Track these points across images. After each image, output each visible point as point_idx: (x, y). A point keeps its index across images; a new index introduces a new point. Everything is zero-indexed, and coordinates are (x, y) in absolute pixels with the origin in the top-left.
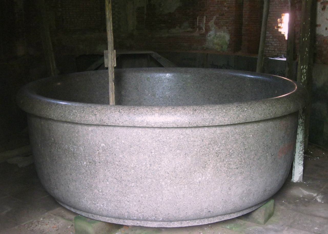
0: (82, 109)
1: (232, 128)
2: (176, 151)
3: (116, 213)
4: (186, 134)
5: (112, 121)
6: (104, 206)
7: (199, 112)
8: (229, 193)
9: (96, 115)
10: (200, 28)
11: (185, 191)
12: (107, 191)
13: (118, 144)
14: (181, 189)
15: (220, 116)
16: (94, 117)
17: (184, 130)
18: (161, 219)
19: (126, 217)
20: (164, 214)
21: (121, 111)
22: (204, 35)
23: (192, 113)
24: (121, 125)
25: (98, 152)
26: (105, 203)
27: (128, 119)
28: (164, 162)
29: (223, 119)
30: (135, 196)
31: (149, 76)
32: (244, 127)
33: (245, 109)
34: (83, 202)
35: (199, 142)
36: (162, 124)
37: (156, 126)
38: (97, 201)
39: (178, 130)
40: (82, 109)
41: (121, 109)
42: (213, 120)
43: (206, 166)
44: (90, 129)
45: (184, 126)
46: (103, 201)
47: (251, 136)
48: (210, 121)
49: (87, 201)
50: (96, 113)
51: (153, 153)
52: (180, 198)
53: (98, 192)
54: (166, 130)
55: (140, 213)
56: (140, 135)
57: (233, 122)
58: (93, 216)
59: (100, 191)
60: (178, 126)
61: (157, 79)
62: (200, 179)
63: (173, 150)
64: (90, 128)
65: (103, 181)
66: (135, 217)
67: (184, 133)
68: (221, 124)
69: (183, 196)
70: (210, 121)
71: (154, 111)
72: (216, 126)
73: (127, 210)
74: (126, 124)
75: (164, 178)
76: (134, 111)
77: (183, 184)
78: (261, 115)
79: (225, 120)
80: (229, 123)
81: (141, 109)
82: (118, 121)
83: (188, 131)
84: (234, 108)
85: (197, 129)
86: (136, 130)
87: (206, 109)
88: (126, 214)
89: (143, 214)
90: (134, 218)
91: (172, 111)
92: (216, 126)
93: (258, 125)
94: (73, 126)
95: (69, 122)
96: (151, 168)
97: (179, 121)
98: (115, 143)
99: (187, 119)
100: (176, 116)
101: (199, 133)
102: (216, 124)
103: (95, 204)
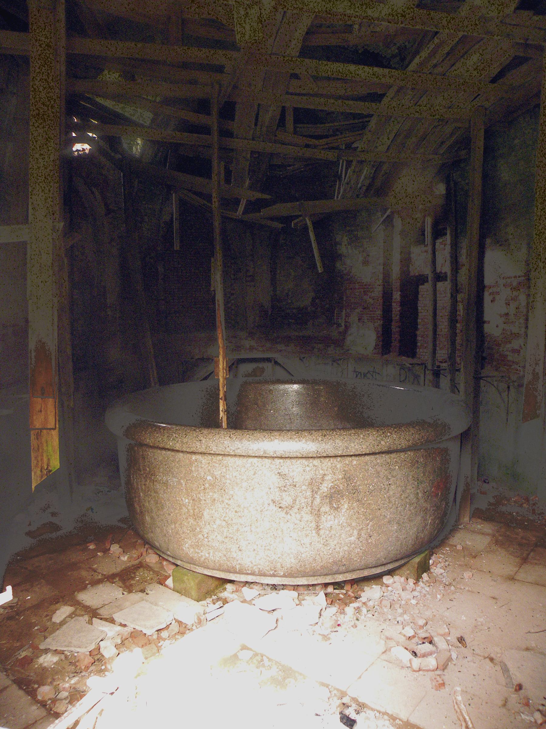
0: (184, 433)
4: (314, 466)
10: (339, 325)
12: (214, 537)
13: (228, 476)
14: (307, 536)
15: (355, 443)
16: (198, 444)
17: (311, 460)
18: (282, 574)
20: (286, 568)
22: (345, 333)
23: (320, 439)
24: (232, 453)
26: (211, 551)
27: (240, 447)
28: (286, 501)
31: (271, 388)
33: (389, 434)
34: (183, 550)
35: (330, 475)
36: (283, 453)
37: (275, 455)
38: (202, 548)
39: (304, 461)
40: (184, 433)
42: (347, 448)
44: (194, 458)
45: (310, 455)
47: (397, 467)
48: (344, 449)
49: (187, 548)
53: (202, 538)
54: (288, 461)
55: (255, 565)
56: (256, 466)
57: (373, 450)
59: (205, 536)
61: (281, 392)
62: (331, 522)
63: (297, 486)
64: (194, 457)
65: (209, 524)
66: (248, 570)
67: (311, 465)
68: (357, 453)
70: (344, 449)
71: (273, 436)
72: (351, 456)
73: (239, 562)
74: (239, 452)
77: (310, 529)
80: (368, 452)
81: (257, 434)
82: (228, 449)
83: (316, 462)
84: (374, 433)
85: (328, 459)
86: (251, 460)
87: (338, 434)
88: (238, 567)
92: (351, 456)
93: (406, 454)
94: (173, 453)
95: (169, 450)
97: (305, 449)
101: (329, 464)
102: (351, 454)
103: (198, 553)
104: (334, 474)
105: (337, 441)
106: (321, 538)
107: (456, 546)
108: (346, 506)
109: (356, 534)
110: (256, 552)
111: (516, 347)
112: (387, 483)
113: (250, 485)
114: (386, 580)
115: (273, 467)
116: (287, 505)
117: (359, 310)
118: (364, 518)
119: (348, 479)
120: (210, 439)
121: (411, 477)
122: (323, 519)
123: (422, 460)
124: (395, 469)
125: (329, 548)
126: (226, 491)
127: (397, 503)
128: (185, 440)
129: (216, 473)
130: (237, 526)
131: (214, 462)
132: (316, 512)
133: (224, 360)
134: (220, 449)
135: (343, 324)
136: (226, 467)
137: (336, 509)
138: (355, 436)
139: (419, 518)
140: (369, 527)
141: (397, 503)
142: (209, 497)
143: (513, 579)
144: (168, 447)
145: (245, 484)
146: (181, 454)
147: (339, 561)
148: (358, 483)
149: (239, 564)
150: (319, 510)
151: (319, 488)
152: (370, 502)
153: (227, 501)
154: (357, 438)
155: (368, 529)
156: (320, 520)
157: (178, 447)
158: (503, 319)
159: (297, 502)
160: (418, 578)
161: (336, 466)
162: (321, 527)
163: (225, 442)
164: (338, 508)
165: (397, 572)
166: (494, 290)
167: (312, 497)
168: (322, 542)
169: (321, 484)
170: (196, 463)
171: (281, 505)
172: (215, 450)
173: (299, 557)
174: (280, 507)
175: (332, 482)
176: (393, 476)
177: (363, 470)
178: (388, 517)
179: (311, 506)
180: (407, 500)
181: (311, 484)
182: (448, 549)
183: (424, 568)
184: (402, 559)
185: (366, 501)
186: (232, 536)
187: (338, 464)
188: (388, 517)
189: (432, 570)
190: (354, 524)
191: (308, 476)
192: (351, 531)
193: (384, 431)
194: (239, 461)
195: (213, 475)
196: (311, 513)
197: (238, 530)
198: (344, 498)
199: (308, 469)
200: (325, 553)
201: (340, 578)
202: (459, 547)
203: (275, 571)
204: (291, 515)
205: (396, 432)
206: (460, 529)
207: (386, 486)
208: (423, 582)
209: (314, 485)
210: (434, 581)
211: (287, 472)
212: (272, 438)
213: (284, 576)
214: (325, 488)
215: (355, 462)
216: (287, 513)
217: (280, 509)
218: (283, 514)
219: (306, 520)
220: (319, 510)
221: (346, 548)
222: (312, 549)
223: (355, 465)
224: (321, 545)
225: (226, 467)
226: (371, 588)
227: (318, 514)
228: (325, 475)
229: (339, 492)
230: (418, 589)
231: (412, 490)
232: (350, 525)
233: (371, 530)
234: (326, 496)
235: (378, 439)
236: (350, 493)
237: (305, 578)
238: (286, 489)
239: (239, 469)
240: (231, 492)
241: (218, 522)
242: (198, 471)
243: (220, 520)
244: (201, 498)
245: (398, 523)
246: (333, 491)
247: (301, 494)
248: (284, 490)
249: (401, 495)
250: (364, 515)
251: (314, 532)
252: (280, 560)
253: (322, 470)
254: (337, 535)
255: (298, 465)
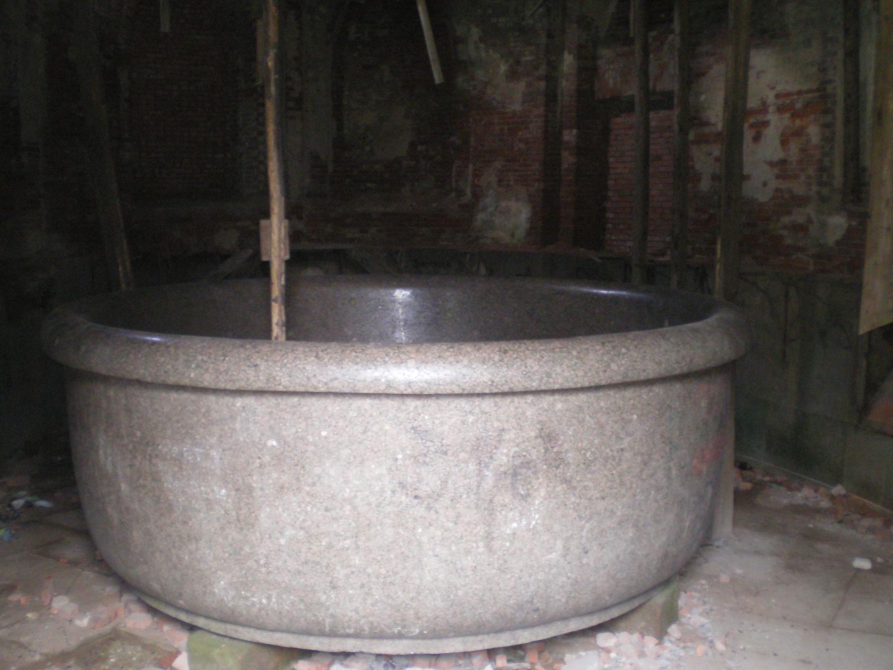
0: (220, 353)
1: (591, 396)
2: (458, 455)
3: (302, 620)
4: (483, 413)
5: (298, 381)
6: (269, 604)
7: (515, 356)
8: (585, 561)
9: (256, 366)
10: (460, 193)
11: (478, 557)
12: (280, 564)
13: (310, 438)
14: (467, 552)
15: (564, 366)
16: (251, 373)
17: (477, 401)
18: (417, 631)
19: (327, 629)
20: (425, 619)
21: (320, 353)
22: (471, 208)
23: (497, 358)
24: (323, 390)
25: (258, 461)
26: (274, 594)
27: (339, 375)
28: (427, 484)
29: (573, 373)
30: (353, 572)
31: (353, 295)
32: (617, 396)
33: (624, 350)
34: (214, 593)
35: (514, 431)
36: (426, 385)
37: (409, 391)
38: (254, 588)
39: (463, 403)
40: (220, 353)
41: (322, 351)
42: (549, 375)
43: (531, 492)
44: (238, 405)
45: (478, 390)
46: (269, 589)
47: (635, 417)
48: (542, 378)
49: (222, 589)
50: (258, 362)
51: (400, 462)
52: (467, 576)
53: (255, 566)
54: (432, 403)
55: (364, 617)
56: (367, 415)
57: (597, 380)
58: (236, 631)
59: (262, 562)
60: (464, 390)
61: (372, 302)
62: (515, 525)
63: (450, 453)
64: (239, 402)
65: (270, 538)
66: (349, 627)
67: (477, 411)
68: (567, 385)
69: (473, 571)
70: (542, 378)
71: (403, 353)
72: (553, 392)
73: (331, 611)
74: (337, 386)
75: (427, 524)
76: (354, 354)
77: (474, 539)
78: (659, 363)
79: (577, 376)
81: (372, 349)
82: (314, 381)
83: (487, 404)
84: (598, 348)
85: (508, 400)
86: (358, 402)
87: (530, 348)
88: (328, 621)
89: (370, 619)
90: (348, 631)
91: (448, 354)
92: (553, 392)
93: (650, 391)
94: (193, 397)
96: (394, 499)
97: (467, 378)
98: (302, 439)
99: (485, 373)
100: (459, 366)
101: (512, 409)
102: (556, 387)
103: (247, 598)
104: (521, 429)
105: (529, 362)
106: (496, 557)
107: (717, 577)
108: (543, 493)
109: (561, 547)
110: (366, 590)
111: (801, 220)
112: (618, 447)
113: (355, 453)
114: (604, 639)
115: (403, 416)
116: (430, 492)
117: (497, 165)
118: (575, 515)
119: (548, 437)
120: (275, 362)
121: (658, 437)
122: (500, 517)
123: (677, 403)
124: (631, 421)
125: (509, 576)
126: (307, 467)
127: (634, 485)
128: (223, 366)
129: (284, 433)
130: (327, 539)
131: (282, 410)
132: (486, 506)
133: (281, 223)
134: (297, 382)
136: (306, 419)
137: (525, 497)
138: (562, 352)
139: (671, 516)
140: (584, 533)
141: (634, 485)
142: (270, 481)
143: (831, 626)
144: (186, 382)
145: (345, 452)
146: (212, 398)
147: (527, 602)
148: (566, 446)
149: (332, 616)
150: (491, 501)
151: (491, 457)
152: (586, 483)
153: (307, 489)
154: (565, 357)
155: (581, 537)
156: (494, 519)
157: (207, 380)
158: (776, 171)
159: (450, 485)
160: (661, 635)
161: (524, 413)
162: (494, 535)
163: (308, 367)
164: (528, 495)
165: (622, 624)
166: (760, 118)
167: (478, 475)
168: (496, 566)
169: (496, 448)
170: (244, 414)
171: (417, 493)
172: (287, 383)
173: (452, 597)
174: (416, 497)
175: (518, 445)
176: (628, 434)
177: (574, 421)
178: (619, 513)
179: (476, 494)
180: (652, 482)
181: (476, 449)
182: (704, 582)
183: (671, 615)
184: (633, 598)
185: (579, 482)
186: (318, 559)
187: (528, 407)
188: (619, 513)
189: (683, 620)
190: (557, 527)
191: (471, 434)
192: (552, 541)
193: (614, 344)
194: (334, 406)
195: (280, 439)
196: (476, 508)
197: (330, 546)
198: (540, 475)
199: (471, 419)
200: (502, 585)
201: (524, 637)
202: (724, 578)
203: (404, 627)
204: (437, 512)
205: (636, 347)
206: (718, 547)
207: (615, 453)
208: (671, 642)
209: (481, 450)
210: (690, 637)
211: (430, 426)
212: (403, 357)
213: (421, 636)
214: (503, 457)
215: (559, 406)
216: (429, 508)
217: (416, 501)
218: (420, 511)
219: (467, 520)
220: (491, 501)
221: (541, 576)
222: (478, 578)
223: (560, 411)
224: (494, 571)
225: (306, 419)
226: (579, 657)
227: (489, 509)
228: (503, 430)
229: (527, 464)
230: (666, 653)
231: (661, 461)
232: (549, 530)
233: (588, 539)
234: (505, 473)
235: (605, 359)
236: (550, 466)
237: (460, 639)
238: (428, 460)
239: (333, 423)
240: (317, 470)
241: (290, 532)
242: (248, 429)
243: (293, 526)
244: (254, 485)
245: (635, 526)
246: (518, 462)
247: (457, 469)
248: (425, 462)
249: (641, 471)
250: (574, 509)
251: (481, 544)
252: (414, 604)
253: (498, 420)
254: (525, 550)
255: (453, 411)
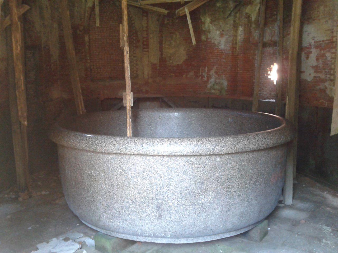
0: (103, 140)
1: (230, 157)
2: (182, 176)
3: (131, 230)
5: (128, 150)
6: (120, 224)
7: (202, 143)
8: (228, 213)
9: (114, 145)
10: (203, 77)
11: (190, 211)
16: (113, 147)
18: (170, 236)
19: (139, 234)
20: (172, 232)
21: (136, 141)
23: (195, 143)
25: (116, 176)
27: (141, 149)
29: (222, 148)
30: (147, 215)
31: (160, 115)
32: (240, 156)
33: (241, 141)
34: (102, 220)
36: (170, 153)
37: (165, 155)
40: (103, 140)
41: (136, 140)
42: (214, 149)
43: (208, 189)
45: (189, 154)
46: (120, 220)
49: (105, 220)
50: (115, 143)
51: (163, 178)
52: (186, 217)
53: (115, 212)
55: (151, 230)
58: (110, 233)
59: (117, 210)
60: (183, 154)
63: (180, 175)
66: (146, 233)
69: (188, 216)
72: (216, 155)
75: (172, 199)
76: (147, 141)
77: (189, 205)
78: (255, 145)
79: (224, 150)
80: (227, 153)
82: (133, 150)
84: (232, 140)
88: (139, 231)
89: (154, 231)
90: (146, 235)
91: (178, 142)
95: (92, 152)
96: (161, 190)
98: (130, 169)
99: (191, 149)
100: (182, 146)
103: (113, 222)
117: (215, 68)
135: (206, 76)
149: (141, 229)
